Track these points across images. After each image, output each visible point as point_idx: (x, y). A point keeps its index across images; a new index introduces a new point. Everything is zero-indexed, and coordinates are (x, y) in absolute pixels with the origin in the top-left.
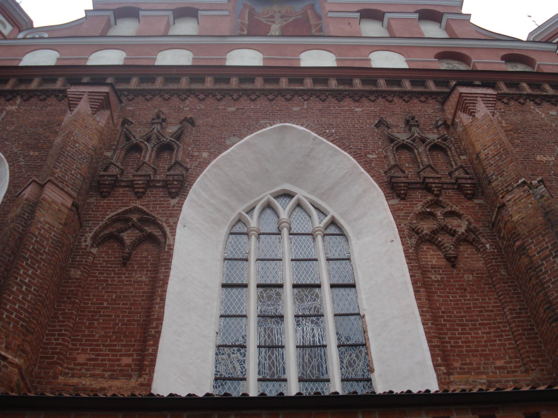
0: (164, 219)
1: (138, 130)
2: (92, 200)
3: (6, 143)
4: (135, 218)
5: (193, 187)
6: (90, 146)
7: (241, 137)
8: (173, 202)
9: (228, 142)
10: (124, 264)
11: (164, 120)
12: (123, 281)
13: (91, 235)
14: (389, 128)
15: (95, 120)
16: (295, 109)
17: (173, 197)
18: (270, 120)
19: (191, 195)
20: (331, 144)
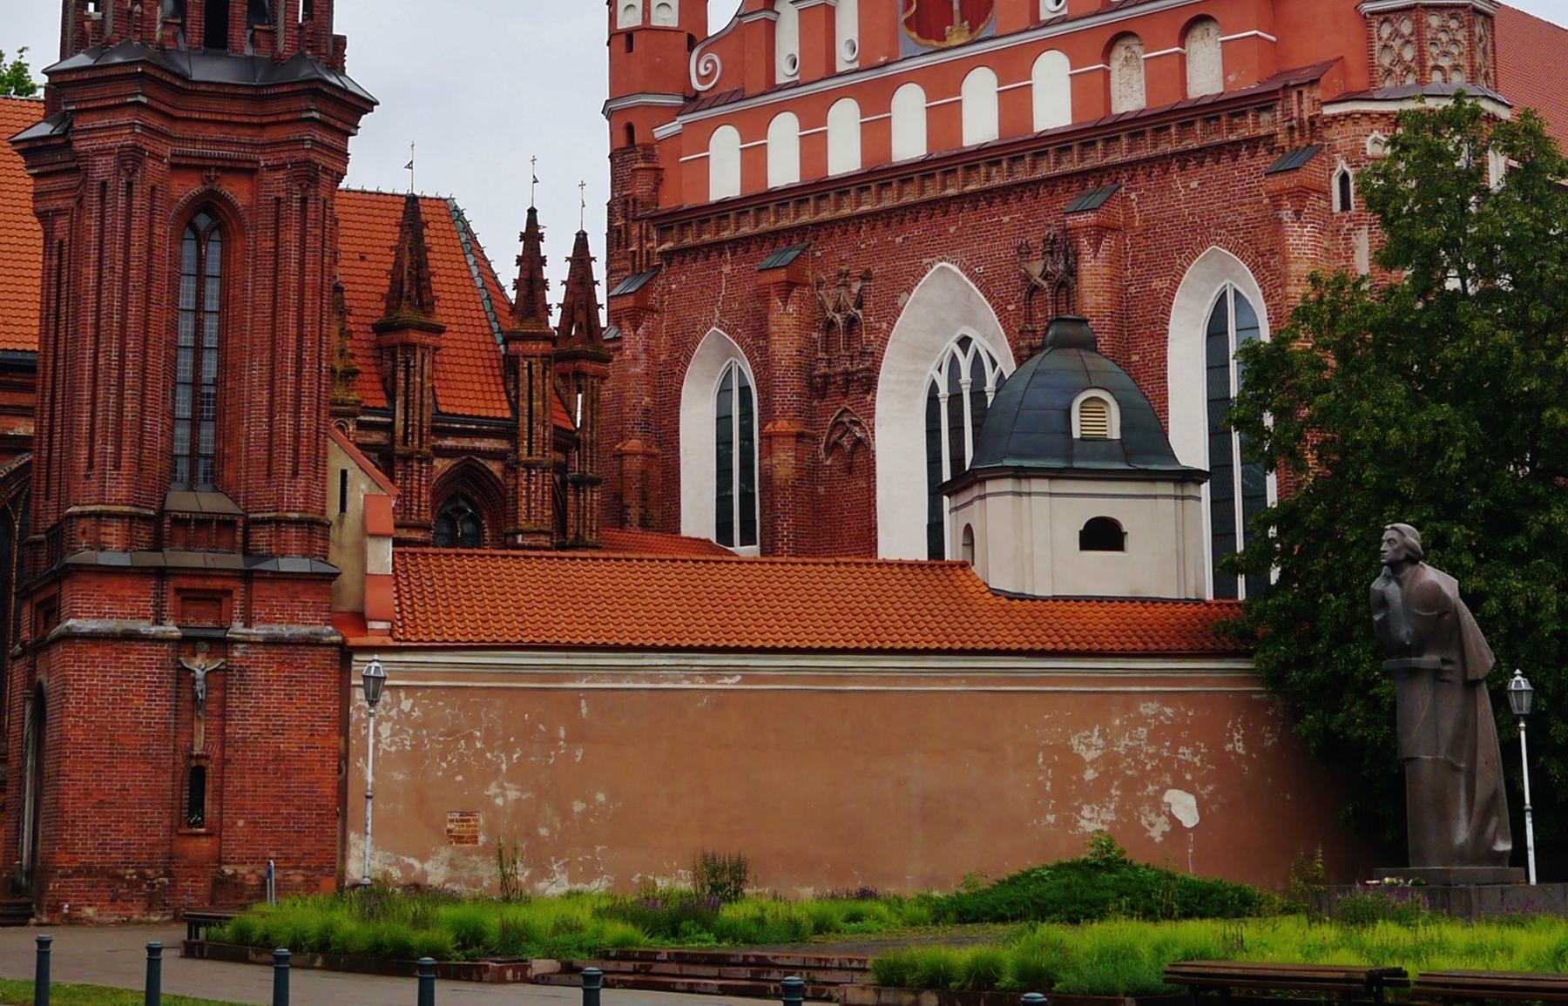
0: (865, 421)
1: (830, 292)
2: (815, 403)
3: (739, 330)
4: (845, 419)
5: (880, 376)
6: (795, 353)
7: (909, 291)
8: (869, 398)
9: (900, 304)
10: (850, 473)
11: (847, 274)
12: (851, 489)
13: (822, 446)
14: (1030, 253)
15: (788, 314)
16: (952, 230)
17: (868, 394)
18: (931, 257)
19: (881, 386)
20: (978, 292)
